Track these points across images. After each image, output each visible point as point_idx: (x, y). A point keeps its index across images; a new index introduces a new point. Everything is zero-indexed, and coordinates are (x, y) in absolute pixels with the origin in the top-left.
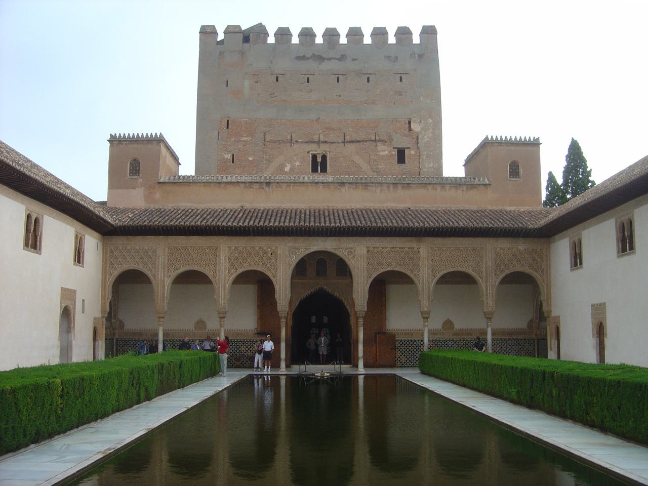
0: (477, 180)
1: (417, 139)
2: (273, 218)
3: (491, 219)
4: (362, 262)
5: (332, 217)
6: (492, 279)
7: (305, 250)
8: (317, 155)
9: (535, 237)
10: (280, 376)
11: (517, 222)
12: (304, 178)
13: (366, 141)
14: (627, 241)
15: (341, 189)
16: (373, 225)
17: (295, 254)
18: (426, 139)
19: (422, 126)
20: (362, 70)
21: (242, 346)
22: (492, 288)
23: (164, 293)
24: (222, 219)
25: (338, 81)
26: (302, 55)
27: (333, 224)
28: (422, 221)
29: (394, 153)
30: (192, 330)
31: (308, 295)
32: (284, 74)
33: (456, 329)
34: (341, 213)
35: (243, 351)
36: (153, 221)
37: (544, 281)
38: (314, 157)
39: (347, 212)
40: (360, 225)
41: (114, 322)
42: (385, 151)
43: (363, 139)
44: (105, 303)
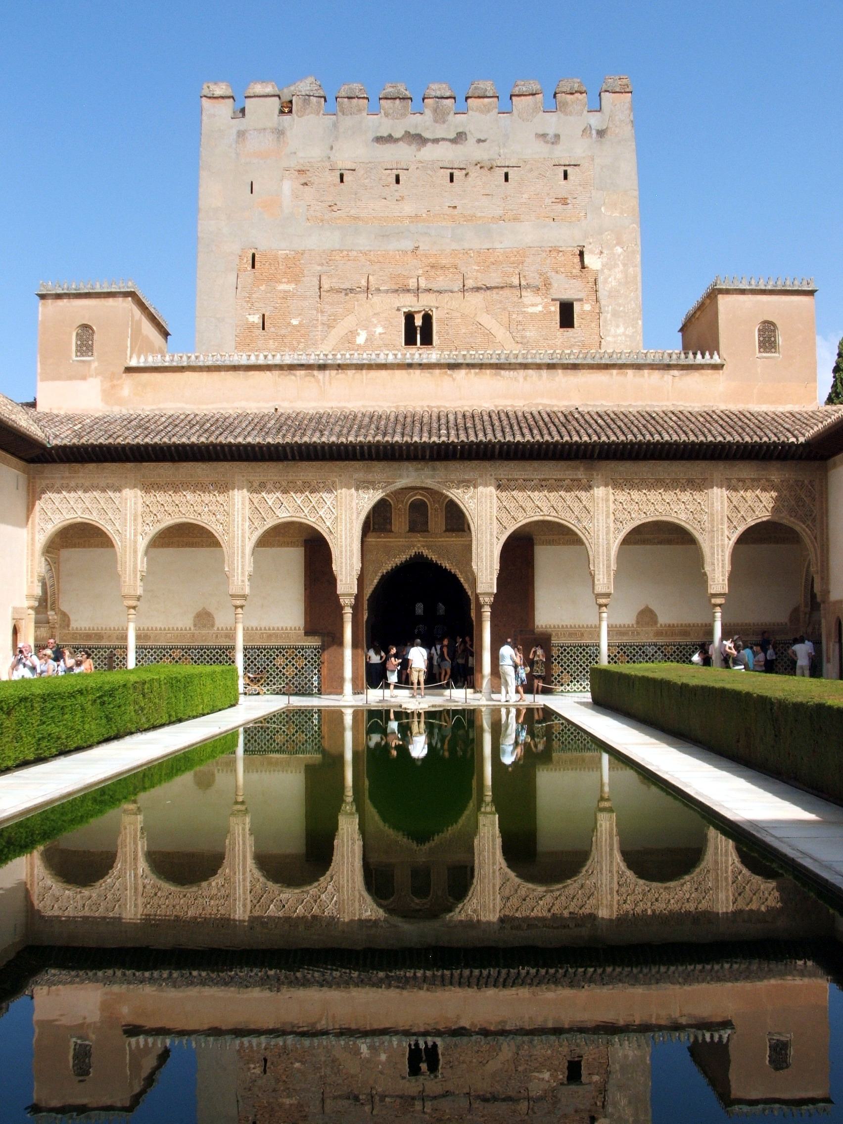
0: (699, 356)
1: (596, 285)
3: (721, 426)
4: (488, 506)
5: (435, 425)
6: (722, 535)
7: (385, 484)
8: (416, 316)
9: (800, 458)
11: (768, 432)
12: (387, 355)
13: (502, 288)
15: (454, 376)
16: (507, 439)
18: (613, 283)
19: (605, 260)
20: (493, 160)
21: (277, 656)
22: (723, 551)
23: (136, 564)
24: (238, 430)
25: (452, 180)
26: (385, 135)
27: (434, 439)
29: (553, 309)
30: (190, 629)
31: (394, 565)
32: (354, 170)
33: (661, 625)
34: (451, 418)
35: (281, 665)
36: (115, 436)
37: (815, 538)
38: (409, 318)
39: (464, 416)
40: (484, 440)
42: (536, 305)
43: (497, 285)
44: (32, 582)
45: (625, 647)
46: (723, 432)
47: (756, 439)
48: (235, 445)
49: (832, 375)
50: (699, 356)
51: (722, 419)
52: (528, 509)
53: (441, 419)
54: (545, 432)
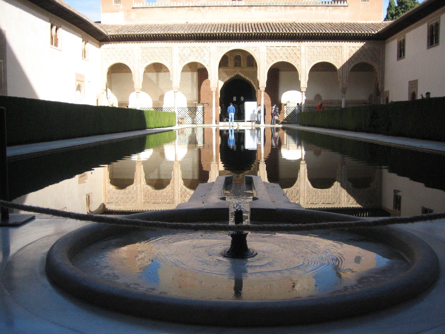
0: (339, 2)
2: (207, 28)
5: (244, 27)
9: (376, 39)
10: (211, 127)
11: (364, 30)
12: (226, 3)
14: (434, 38)
16: (270, 32)
17: (221, 52)
22: (346, 73)
27: (245, 32)
28: (302, 29)
31: (229, 78)
33: (323, 100)
34: (250, 25)
36: (131, 31)
37: (380, 69)
40: (262, 32)
41: (110, 98)
45: (310, 108)
46: (348, 30)
47: (360, 32)
48: (174, 34)
49: (387, 11)
50: (339, 2)
51: (348, 26)
52: (277, 57)
53: (245, 26)
54: (284, 29)
